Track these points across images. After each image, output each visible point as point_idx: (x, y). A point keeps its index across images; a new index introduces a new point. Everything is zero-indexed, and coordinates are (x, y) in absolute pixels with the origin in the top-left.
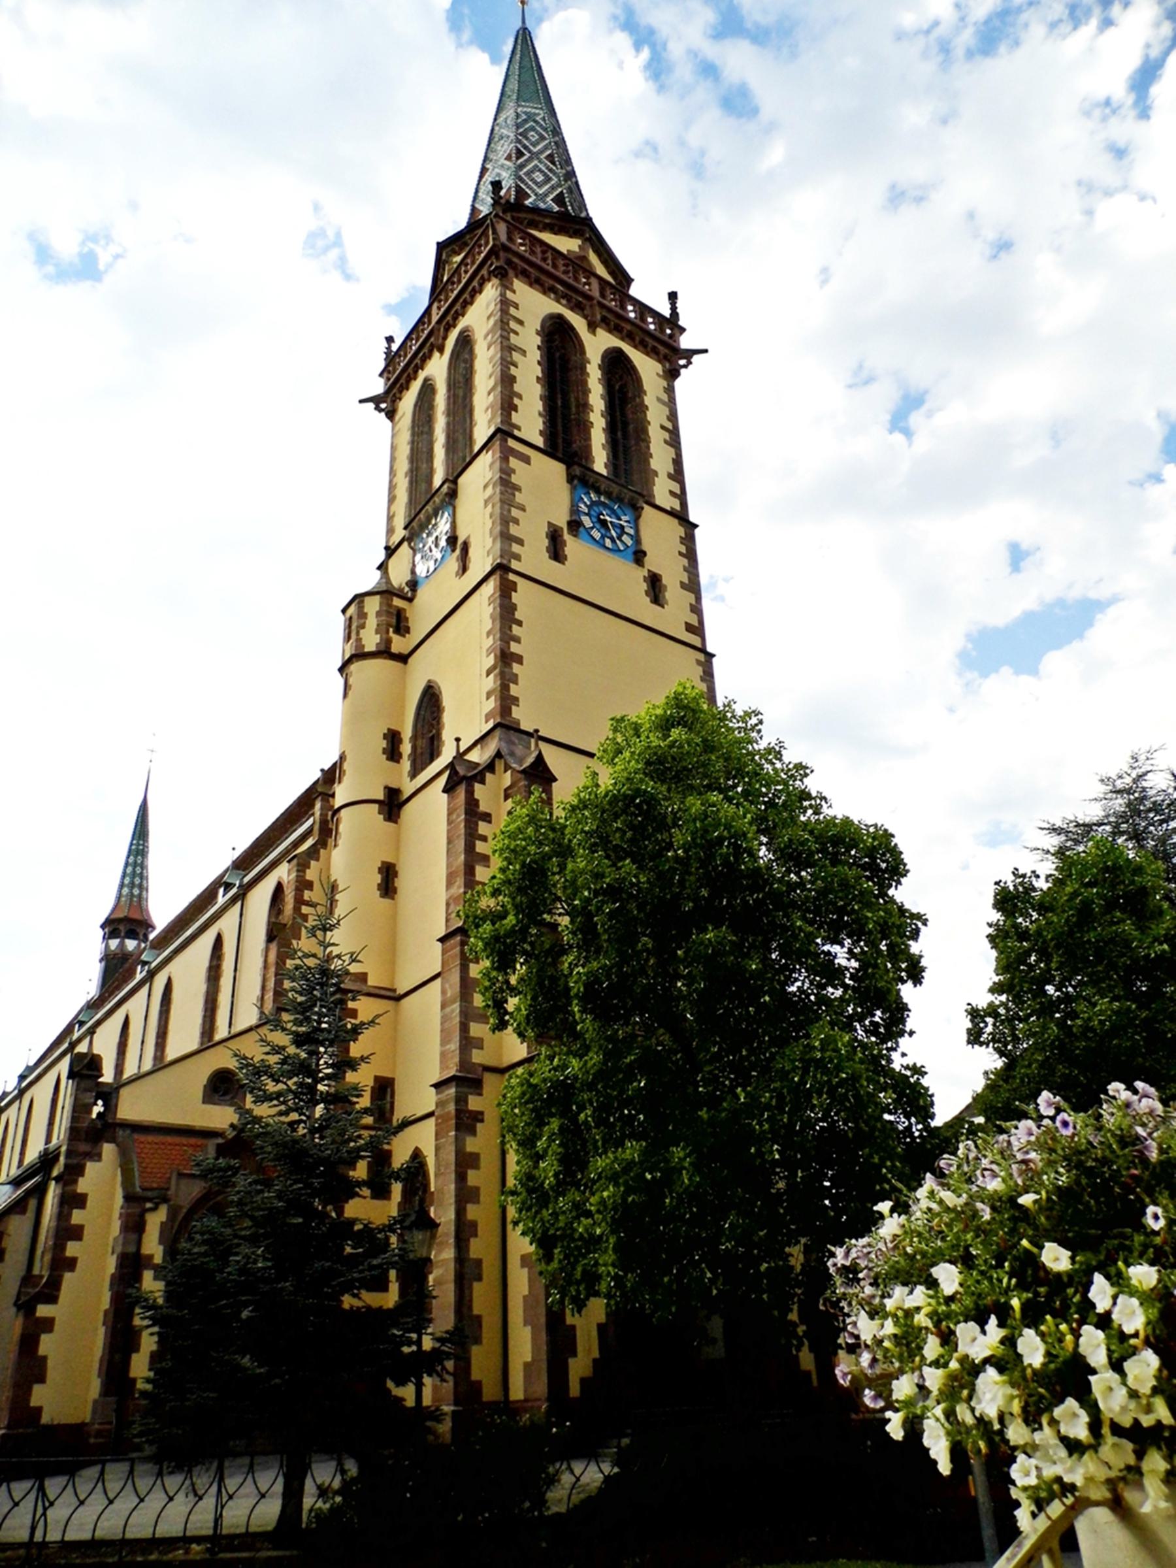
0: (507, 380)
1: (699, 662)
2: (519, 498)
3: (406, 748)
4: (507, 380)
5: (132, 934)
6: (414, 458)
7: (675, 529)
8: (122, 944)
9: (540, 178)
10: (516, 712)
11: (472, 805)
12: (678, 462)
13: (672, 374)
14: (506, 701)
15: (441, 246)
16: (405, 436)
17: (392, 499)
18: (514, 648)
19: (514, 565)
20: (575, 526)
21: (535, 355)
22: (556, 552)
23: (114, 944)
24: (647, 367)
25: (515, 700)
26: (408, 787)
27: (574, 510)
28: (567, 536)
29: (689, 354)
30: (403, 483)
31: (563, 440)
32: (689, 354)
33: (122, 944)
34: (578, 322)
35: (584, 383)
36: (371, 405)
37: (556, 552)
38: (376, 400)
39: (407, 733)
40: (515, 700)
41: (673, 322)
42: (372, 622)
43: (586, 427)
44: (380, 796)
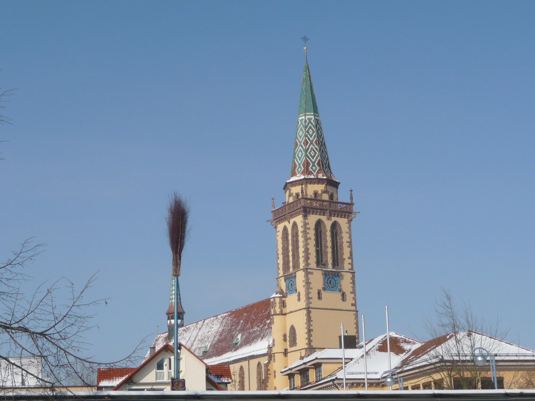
0: (306, 250)
1: (354, 314)
2: (311, 286)
3: (288, 339)
7: (351, 275)
8: (170, 322)
10: (312, 344)
13: (350, 221)
14: (310, 341)
18: (311, 328)
19: (311, 306)
20: (324, 289)
21: (313, 238)
22: (320, 298)
25: (312, 341)
26: (290, 349)
28: (322, 292)
31: (320, 262)
33: (170, 322)
34: (324, 218)
36: (269, 223)
37: (320, 298)
39: (288, 335)
40: (312, 341)
42: (278, 305)
43: (326, 253)
44: (283, 351)
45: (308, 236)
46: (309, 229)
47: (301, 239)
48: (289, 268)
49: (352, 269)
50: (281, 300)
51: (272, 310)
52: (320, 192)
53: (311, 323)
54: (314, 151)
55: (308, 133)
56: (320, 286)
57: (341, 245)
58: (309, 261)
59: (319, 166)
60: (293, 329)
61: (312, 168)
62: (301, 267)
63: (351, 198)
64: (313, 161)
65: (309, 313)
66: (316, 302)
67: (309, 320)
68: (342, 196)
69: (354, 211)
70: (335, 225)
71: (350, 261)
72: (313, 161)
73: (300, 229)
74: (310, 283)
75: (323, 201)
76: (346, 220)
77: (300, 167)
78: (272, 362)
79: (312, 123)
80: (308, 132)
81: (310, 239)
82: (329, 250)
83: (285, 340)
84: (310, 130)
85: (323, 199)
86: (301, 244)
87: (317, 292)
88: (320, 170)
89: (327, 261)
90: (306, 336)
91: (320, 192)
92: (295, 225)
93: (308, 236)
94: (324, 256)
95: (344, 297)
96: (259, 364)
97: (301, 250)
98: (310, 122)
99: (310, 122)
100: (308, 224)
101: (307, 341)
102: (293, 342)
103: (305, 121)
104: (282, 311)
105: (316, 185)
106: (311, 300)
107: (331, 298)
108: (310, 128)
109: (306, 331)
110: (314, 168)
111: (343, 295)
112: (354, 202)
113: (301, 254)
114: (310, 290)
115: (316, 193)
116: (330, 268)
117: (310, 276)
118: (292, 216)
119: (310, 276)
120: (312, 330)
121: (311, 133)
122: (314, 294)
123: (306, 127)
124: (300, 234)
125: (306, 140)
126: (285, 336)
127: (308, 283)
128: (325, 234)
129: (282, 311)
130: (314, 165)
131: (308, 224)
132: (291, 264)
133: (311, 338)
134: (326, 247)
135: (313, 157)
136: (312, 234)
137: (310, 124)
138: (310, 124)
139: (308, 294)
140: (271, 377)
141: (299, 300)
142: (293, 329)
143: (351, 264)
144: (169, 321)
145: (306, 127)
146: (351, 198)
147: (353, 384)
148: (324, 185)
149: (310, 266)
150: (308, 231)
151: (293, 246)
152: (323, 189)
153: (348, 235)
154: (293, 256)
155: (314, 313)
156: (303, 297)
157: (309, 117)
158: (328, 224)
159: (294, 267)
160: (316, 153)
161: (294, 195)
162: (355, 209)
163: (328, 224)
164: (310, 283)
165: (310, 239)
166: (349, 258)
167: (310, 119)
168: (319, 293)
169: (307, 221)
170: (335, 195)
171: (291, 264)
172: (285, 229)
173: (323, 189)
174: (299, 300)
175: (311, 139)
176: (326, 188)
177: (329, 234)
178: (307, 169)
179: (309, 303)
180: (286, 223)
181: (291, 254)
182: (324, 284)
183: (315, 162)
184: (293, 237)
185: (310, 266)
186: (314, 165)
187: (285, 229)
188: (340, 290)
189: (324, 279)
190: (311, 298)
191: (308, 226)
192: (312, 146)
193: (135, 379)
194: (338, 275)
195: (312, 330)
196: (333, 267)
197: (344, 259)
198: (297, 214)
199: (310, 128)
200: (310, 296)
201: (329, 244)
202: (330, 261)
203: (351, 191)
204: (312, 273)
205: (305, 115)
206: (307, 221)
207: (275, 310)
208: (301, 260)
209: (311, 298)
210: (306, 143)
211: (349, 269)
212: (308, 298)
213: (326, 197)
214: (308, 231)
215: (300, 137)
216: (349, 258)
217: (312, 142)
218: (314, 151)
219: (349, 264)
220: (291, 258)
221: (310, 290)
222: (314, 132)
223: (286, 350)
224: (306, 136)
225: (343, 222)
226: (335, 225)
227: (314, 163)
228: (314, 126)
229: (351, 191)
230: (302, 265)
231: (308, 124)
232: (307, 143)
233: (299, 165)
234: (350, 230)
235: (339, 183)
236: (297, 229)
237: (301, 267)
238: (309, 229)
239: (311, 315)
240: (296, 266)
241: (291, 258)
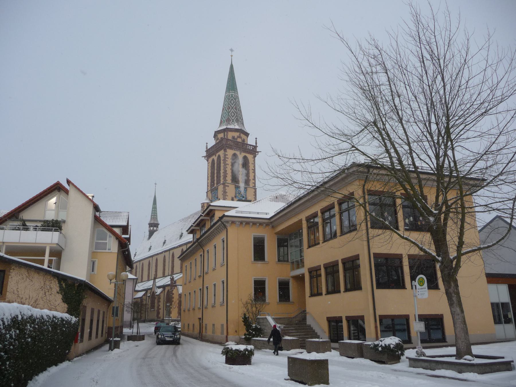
2: (227, 194)
4: (225, 171)
5: (155, 226)
6: (211, 172)
9: (233, 114)
12: (254, 176)
13: (255, 157)
15: (215, 132)
16: (210, 164)
17: (208, 179)
23: (152, 228)
24: (250, 157)
27: (236, 194)
29: (258, 152)
30: (210, 178)
32: (258, 152)
34: (238, 153)
38: (205, 157)
41: (255, 147)
47: (222, 165)
48: (214, 184)
49: (255, 186)
52: (236, 137)
62: (222, 182)
63: (256, 143)
68: (251, 141)
69: (258, 150)
71: (254, 181)
73: (222, 158)
76: (252, 156)
81: (228, 164)
86: (222, 168)
91: (236, 137)
92: (219, 156)
93: (227, 162)
97: (222, 171)
98: (232, 96)
113: (222, 174)
115: (233, 137)
117: (226, 188)
118: (217, 152)
119: (226, 188)
124: (222, 162)
132: (215, 182)
143: (255, 183)
146: (256, 143)
147: (241, 223)
149: (227, 182)
153: (253, 165)
159: (217, 184)
162: (258, 150)
165: (228, 164)
167: (232, 95)
169: (226, 153)
170: (246, 140)
171: (215, 182)
172: (213, 160)
176: (240, 134)
180: (214, 157)
181: (215, 175)
184: (217, 165)
185: (227, 182)
187: (213, 160)
198: (221, 149)
203: (256, 139)
204: (228, 186)
206: (226, 153)
213: (239, 140)
220: (215, 178)
224: (229, 104)
225: (250, 157)
229: (256, 139)
230: (222, 181)
234: (255, 163)
235: (249, 134)
236: (220, 160)
237: (222, 182)
240: (218, 182)
241: (215, 178)
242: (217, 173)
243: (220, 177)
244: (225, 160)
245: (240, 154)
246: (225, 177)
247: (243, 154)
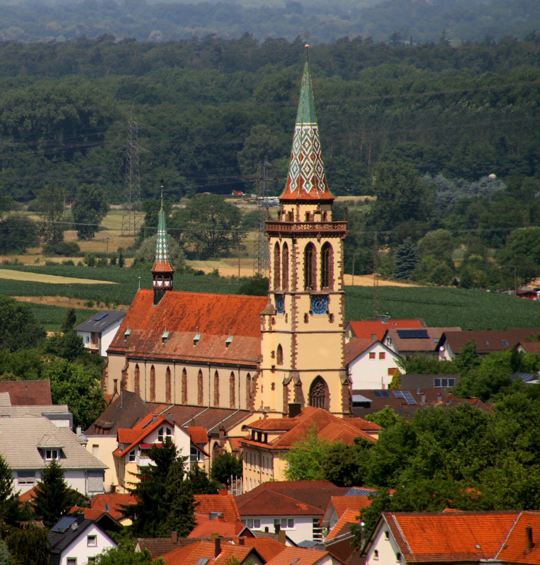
2: (298, 310)
3: (276, 355)
4: (295, 275)
9: (307, 169)
10: (296, 366)
11: (287, 389)
18: (296, 351)
20: (311, 312)
22: (306, 321)
28: (309, 315)
33: (156, 283)
34: (314, 241)
35: (315, 261)
37: (306, 321)
42: (267, 322)
43: (315, 275)
44: (271, 368)
45: (297, 260)
46: (299, 253)
47: (290, 263)
50: (270, 318)
51: (262, 326)
52: (312, 213)
53: (296, 346)
54: (309, 166)
55: (304, 146)
56: (307, 309)
57: (332, 266)
58: (297, 286)
59: (313, 183)
60: (280, 348)
61: (305, 186)
64: (307, 177)
65: (294, 338)
66: (301, 326)
67: (294, 343)
70: (327, 246)
71: (340, 281)
72: (307, 177)
74: (297, 308)
75: (314, 224)
77: (294, 183)
78: (260, 376)
79: (308, 135)
80: (304, 145)
82: (319, 273)
83: (273, 357)
84: (307, 143)
85: (315, 221)
86: (290, 268)
87: (303, 315)
88: (314, 187)
89: (315, 283)
90: (291, 358)
91: (312, 213)
93: (297, 260)
94: (313, 277)
95: (331, 317)
96: (249, 375)
97: (290, 273)
98: (306, 134)
99: (306, 134)
100: (297, 248)
101: (291, 364)
102: (280, 360)
103: (302, 133)
104: (271, 328)
105: (308, 206)
106: (297, 324)
107: (319, 321)
108: (307, 140)
109: (291, 354)
110: (308, 185)
111: (331, 317)
112: (276, 372)
113: (290, 278)
114: (297, 315)
115: (308, 214)
116: (319, 289)
119: (297, 300)
120: (297, 353)
121: (307, 146)
122: (300, 318)
123: (302, 140)
124: (290, 258)
125: (301, 154)
126: (273, 352)
127: (294, 308)
128: (315, 256)
129: (271, 328)
130: (308, 183)
131: (297, 248)
133: (296, 361)
134: (316, 269)
135: (307, 173)
136: (301, 258)
137: (307, 136)
138: (307, 136)
139: (294, 318)
140: (259, 391)
141: (286, 321)
142: (280, 348)
144: (154, 282)
145: (302, 140)
148: (316, 206)
149: (298, 291)
150: (297, 256)
151: (284, 265)
152: (316, 209)
154: (284, 275)
155: (299, 337)
156: (290, 317)
157: (306, 127)
158: (319, 247)
160: (310, 169)
161: (287, 213)
163: (319, 247)
164: (297, 308)
165: (299, 263)
166: (339, 278)
167: (306, 130)
168: (306, 316)
169: (296, 245)
172: (277, 245)
173: (316, 209)
174: (286, 321)
175: (307, 153)
177: (319, 256)
178: (301, 187)
179: (294, 327)
182: (311, 308)
183: (309, 179)
184: (284, 255)
186: (308, 183)
188: (328, 312)
189: (312, 302)
190: (297, 322)
191: (297, 251)
192: (307, 161)
193: (144, 442)
194: (326, 297)
195: (297, 353)
196: (322, 289)
197: (334, 280)
199: (307, 140)
200: (296, 320)
201: (319, 266)
202: (319, 283)
204: (299, 298)
205: (302, 125)
207: (264, 327)
208: (290, 283)
209: (297, 322)
210: (301, 157)
211: (339, 290)
212: (294, 322)
214: (297, 256)
215: (297, 149)
216: (339, 278)
217: (307, 156)
218: (309, 166)
219: (339, 284)
221: (297, 315)
222: (310, 145)
223: (273, 367)
224: (301, 149)
226: (327, 246)
227: (308, 180)
228: (310, 138)
231: (305, 135)
232: (303, 157)
233: (294, 180)
238: (299, 253)
239: (296, 339)
242: (283, 269)
243: (287, 280)
244: (294, 257)
245: (319, 241)
246: (295, 283)
247: (324, 240)
